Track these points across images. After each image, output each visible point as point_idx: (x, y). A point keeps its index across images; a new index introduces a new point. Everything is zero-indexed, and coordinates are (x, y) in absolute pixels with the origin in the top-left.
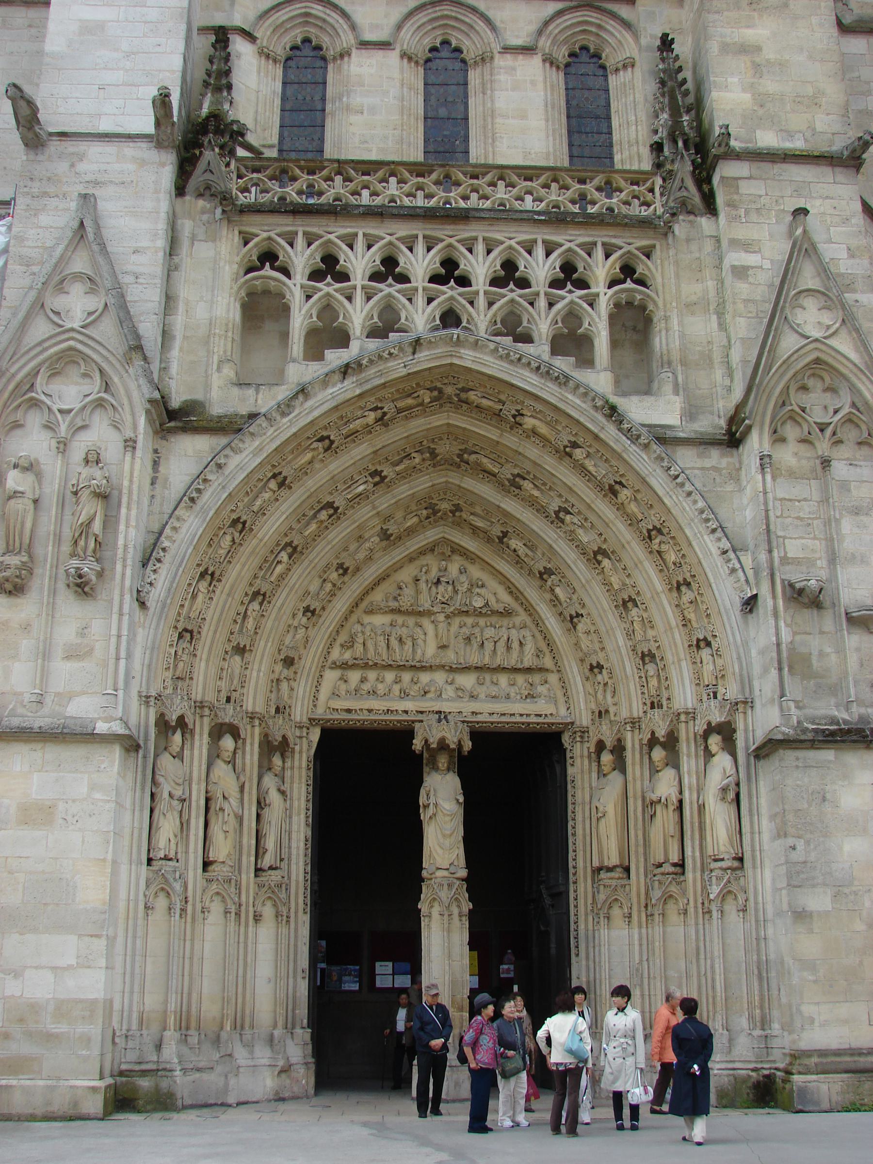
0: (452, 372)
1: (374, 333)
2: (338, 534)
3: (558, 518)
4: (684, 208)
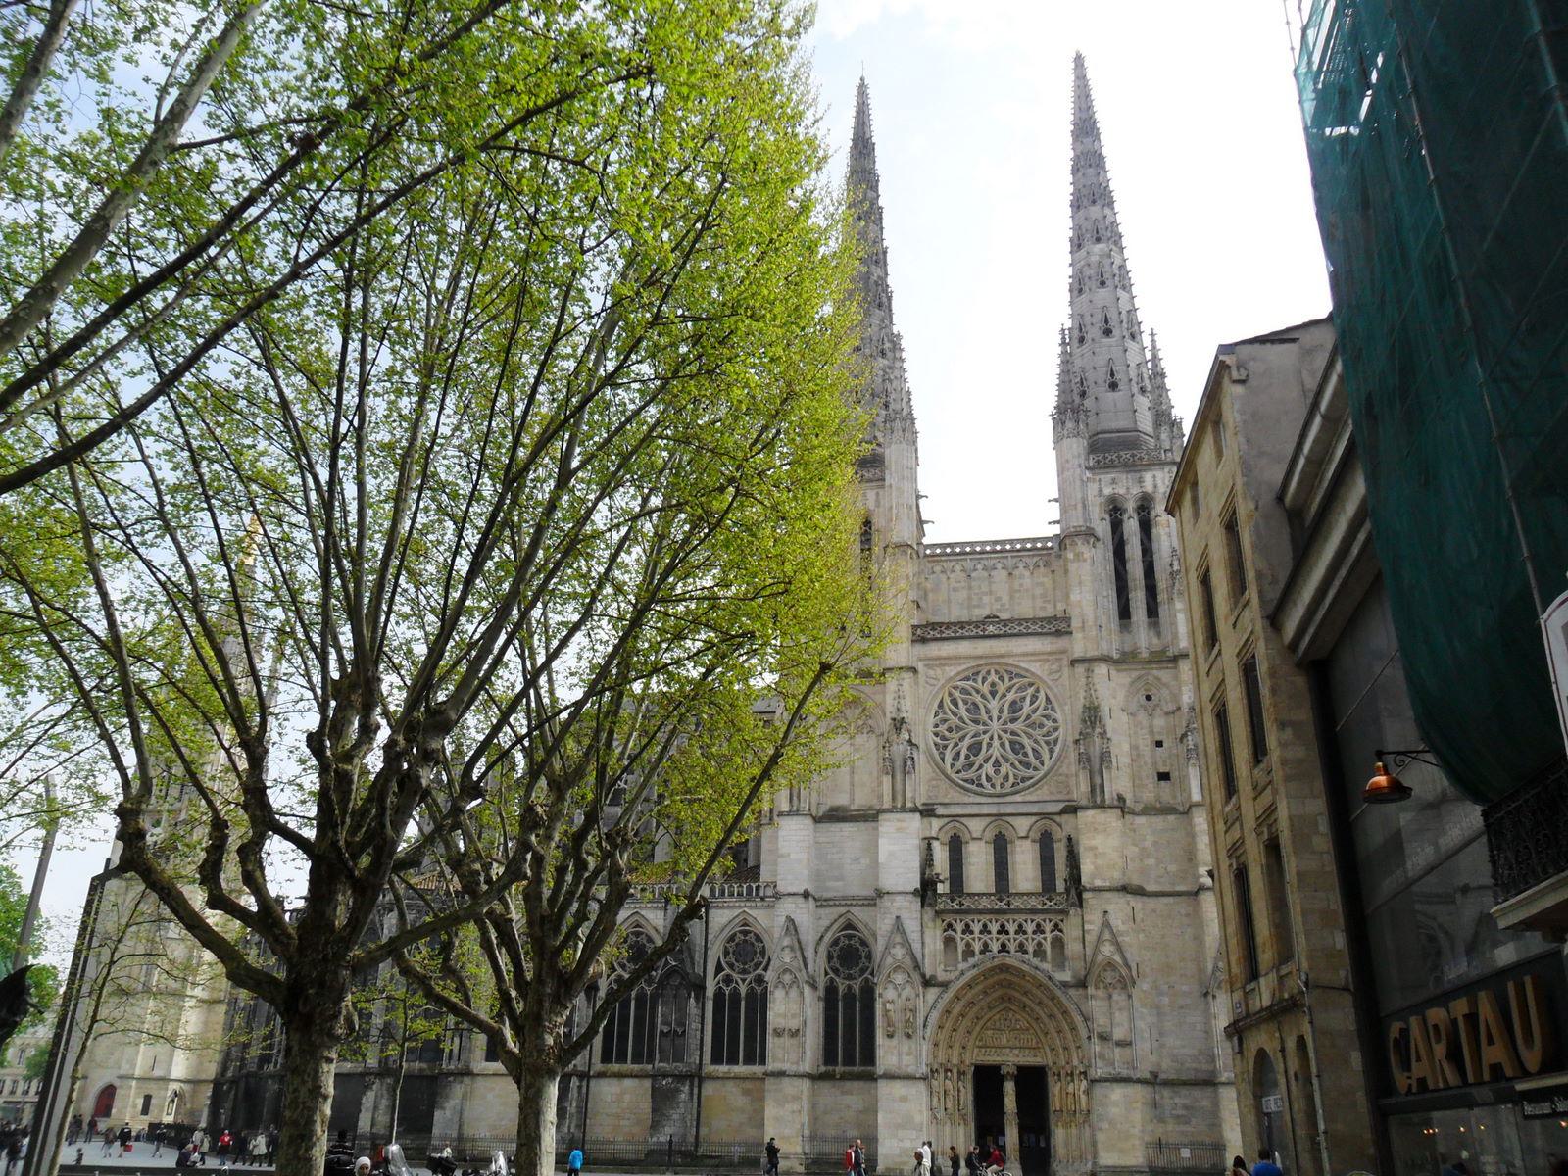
0: (1004, 965)
1: (982, 952)
2: (975, 1009)
3: (1040, 1003)
4: (1073, 904)
